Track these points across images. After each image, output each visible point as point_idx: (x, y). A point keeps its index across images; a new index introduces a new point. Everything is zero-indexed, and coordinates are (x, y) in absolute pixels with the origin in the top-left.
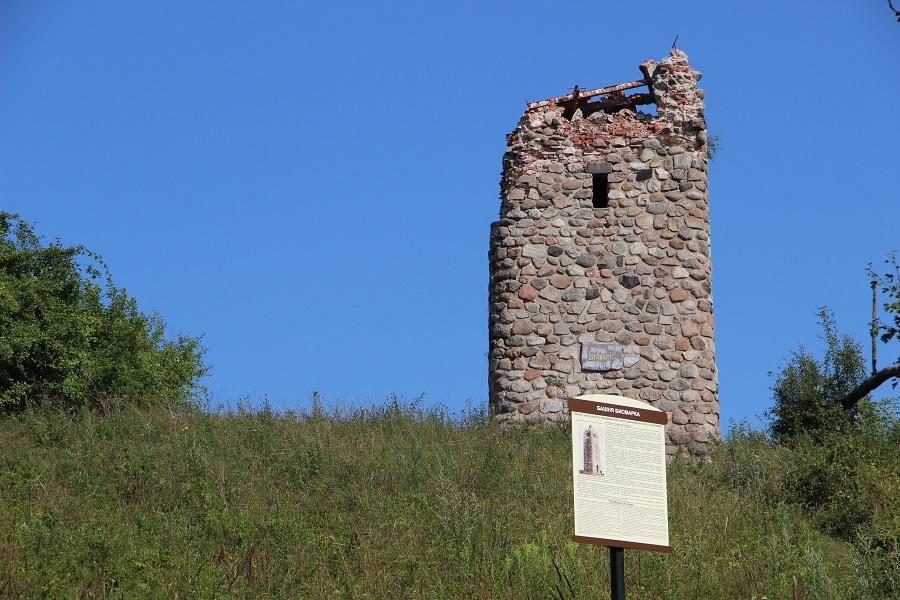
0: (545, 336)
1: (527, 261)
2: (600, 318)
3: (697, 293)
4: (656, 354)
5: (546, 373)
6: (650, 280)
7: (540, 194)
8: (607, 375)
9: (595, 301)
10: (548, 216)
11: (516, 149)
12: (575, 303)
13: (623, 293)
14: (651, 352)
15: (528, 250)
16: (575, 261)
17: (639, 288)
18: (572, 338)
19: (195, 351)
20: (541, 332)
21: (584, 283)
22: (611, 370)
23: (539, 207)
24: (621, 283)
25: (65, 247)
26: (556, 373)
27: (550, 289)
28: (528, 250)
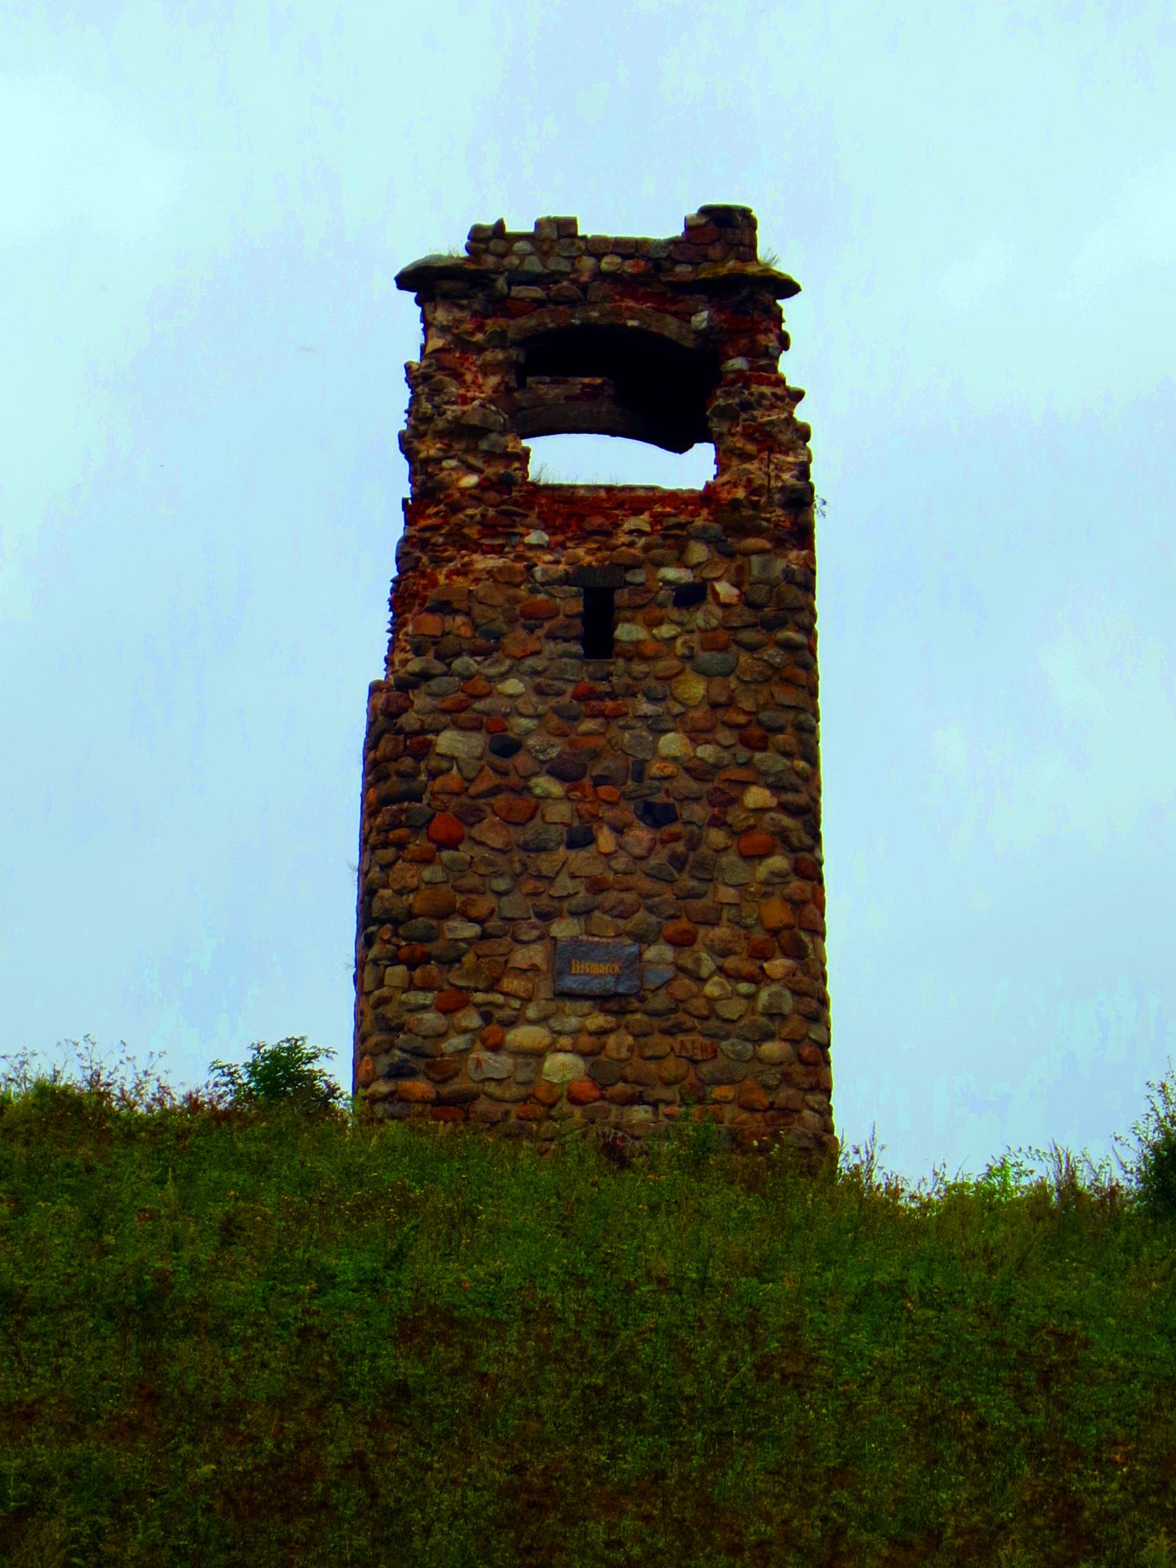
0: (480, 921)
1: (444, 765)
2: (597, 886)
3: (794, 840)
4: (708, 965)
5: (479, 997)
6: (699, 812)
7: (476, 627)
8: (608, 1006)
9: (583, 854)
10: (492, 671)
11: (424, 529)
12: (544, 856)
13: (640, 835)
14: (698, 961)
15: (447, 741)
16: (547, 766)
17: (676, 828)
18: (534, 927)
19: (103, 1078)
20: (662, 992)
21: (559, 812)
22: (616, 995)
23: (473, 654)
24: (639, 817)
25: (307, 1048)
26: (499, 999)
27: (493, 825)
28: (447, 741)
